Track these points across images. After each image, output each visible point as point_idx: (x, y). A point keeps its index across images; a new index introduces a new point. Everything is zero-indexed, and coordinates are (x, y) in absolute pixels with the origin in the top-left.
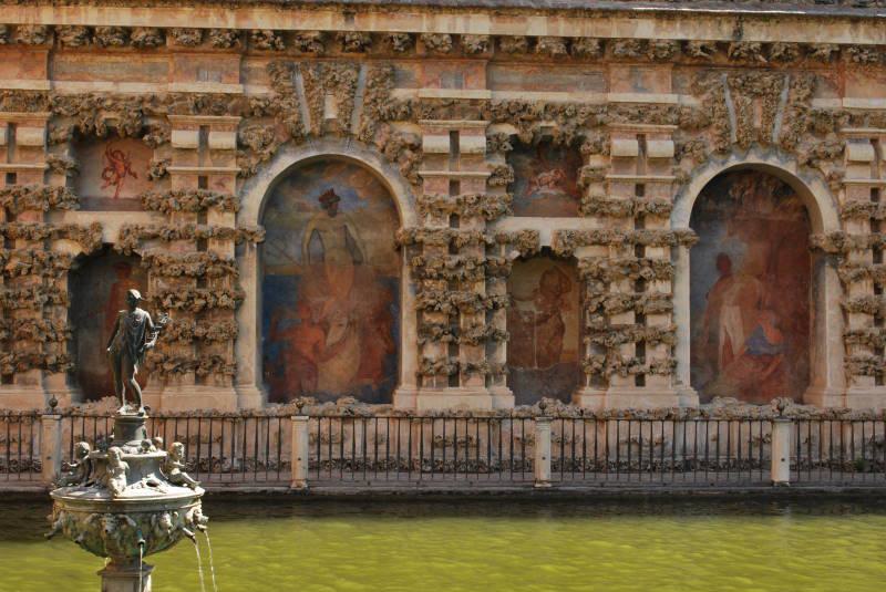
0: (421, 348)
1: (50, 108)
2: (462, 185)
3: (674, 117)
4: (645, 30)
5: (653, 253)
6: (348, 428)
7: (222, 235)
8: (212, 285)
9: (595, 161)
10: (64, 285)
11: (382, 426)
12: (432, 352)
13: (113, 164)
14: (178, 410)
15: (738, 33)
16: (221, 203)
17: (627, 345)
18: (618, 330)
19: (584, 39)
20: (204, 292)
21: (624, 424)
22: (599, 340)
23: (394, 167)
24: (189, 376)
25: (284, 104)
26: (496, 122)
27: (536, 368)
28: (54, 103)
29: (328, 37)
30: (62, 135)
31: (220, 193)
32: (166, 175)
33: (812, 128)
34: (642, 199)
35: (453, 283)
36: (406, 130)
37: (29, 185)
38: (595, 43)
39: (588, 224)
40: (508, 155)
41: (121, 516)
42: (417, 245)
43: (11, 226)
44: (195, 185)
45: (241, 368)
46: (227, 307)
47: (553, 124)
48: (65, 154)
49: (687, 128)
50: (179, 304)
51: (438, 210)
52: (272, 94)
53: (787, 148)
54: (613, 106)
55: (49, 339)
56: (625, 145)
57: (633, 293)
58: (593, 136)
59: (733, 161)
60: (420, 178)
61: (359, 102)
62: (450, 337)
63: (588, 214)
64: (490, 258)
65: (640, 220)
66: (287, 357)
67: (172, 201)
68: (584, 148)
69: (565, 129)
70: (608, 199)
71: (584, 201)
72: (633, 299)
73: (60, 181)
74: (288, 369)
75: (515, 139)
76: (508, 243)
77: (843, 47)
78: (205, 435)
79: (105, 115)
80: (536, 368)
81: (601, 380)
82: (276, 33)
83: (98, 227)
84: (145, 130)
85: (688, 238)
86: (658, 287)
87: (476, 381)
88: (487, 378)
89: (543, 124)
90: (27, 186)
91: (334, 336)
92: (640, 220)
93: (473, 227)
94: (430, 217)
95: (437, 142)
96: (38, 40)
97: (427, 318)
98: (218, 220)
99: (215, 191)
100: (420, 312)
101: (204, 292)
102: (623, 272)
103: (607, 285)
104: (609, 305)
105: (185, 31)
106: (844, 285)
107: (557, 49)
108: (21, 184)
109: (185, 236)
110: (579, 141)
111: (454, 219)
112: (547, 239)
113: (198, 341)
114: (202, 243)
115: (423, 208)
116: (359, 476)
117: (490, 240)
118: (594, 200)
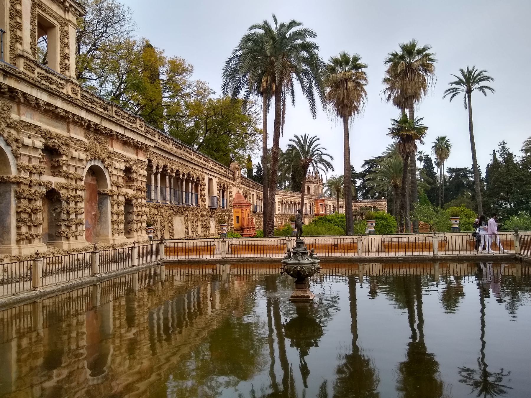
4: (83, 114)
9: (64, 158)
12: (24, 230)
15: (101, 122)
22: (66, 223)
23: (10, 148)
26: (42, 137)
33: (108, 157)
35: (30, 200)
38: (71, 115)
42: (18, 184)
47: (56, 141)
49: (86, 151)
53: (103, 162)
54: (71, 138)
57: (75, 207)
58: (64, 147)
59: (93, 164)
60: (20, 154)
70: (70, 172)
77: (117, 133)
81: (67, 238)
86: (80, 205)
94: (23, 172)
97: (24, 216)
100: (18, 213)
103: (68, 203)
104: (71, 211)
106: (112, 205)
111: (31, 173)
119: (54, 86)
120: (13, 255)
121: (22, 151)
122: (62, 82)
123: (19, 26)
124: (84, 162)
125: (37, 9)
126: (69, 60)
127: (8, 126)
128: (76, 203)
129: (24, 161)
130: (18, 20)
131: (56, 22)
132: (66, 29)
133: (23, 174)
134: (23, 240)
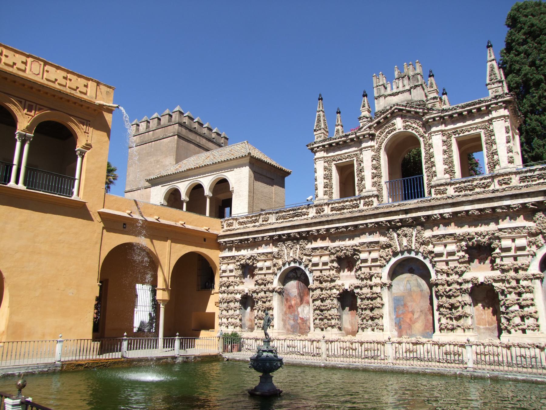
0: (439, 320)
1: (330, 251)
2: (449, 263)
3: (526, 231)
5: (522, 283)
6: (418, 346)
7: (375, 286)
8: (374, 301)
9: (498, 251)
10: (335, 301)
11: (429, 345)
12: (444, 321)
13: (349, 265)
14: (366, 340)
16: (376, 275)
17: (515, 318)
18: (512, 312)
19: (484, 209)
20: (372, 302)
21: (518, 349)
24: (370, 329)
25: (391, 243)
27: (487, 326)
29: (401, 220)
30: (333, 259)
31: (375, 272)
32: (360, 268)
34: (515, 262)
36: (430, 247)
37: (325, 274)
39: (497, 274)
40: (466, 252)
42: (437, 285)
44: (368, 269)
45: (384, 328)
46: (379, 308)
47: (479, 238)
48: (335, 264)
50: (365, 306)
51: (442, 272)
52: (388, 239)
54: (500, 230)
55: (332, 318)
56: (506, 243)
60: (435, 262)
61: (414, 239)
62: (450, 315)
63: (496, 270)
64: (461, 287)
65: (516, 270)
66: (402, 323)
67: (363, 276)
68: (492, 246)
69: (484, 240)
71: (494, 264)
72: (518, 300)
73: (333, 272)
74: (402, 326)
75: (467, 246)
76: (468, 282)
78: (376, 348)
79: (343, 252)
80: (487, 326)
82: (386, 221)
83: (343, 285)
84: (355, 254)
85: (538, 276)
86: (524, 296)
87: (459, 331)
88: (464, 331)
89: (476, 239)
91: (416, 316)
92: (516, 270)
93: (455, 277)
95: (438, 249)
96: (325, 233)
97: (441, 309)
98: (375, 281)
99: (374, 271)
101: (372, 302)
102: (511, 290)
103: (506, 296)
105: (362, 224)
107: (476, 213)
109: (366, 286)
110: (491, 243)
111: (448, 275)
112: (481, 280)
113: (372, 319)
114: (371, 287)
115: (437, 272)
116: (423, 363)
117: (460, 281)
118: (497, 265)
119: (477, 190)
120: (433, 340)
121: (436, 259)
122: (488, 180)
123: (433, 165)
124: (534, 248)
125: (453, 136)
126: (497, 155)
127: (423, 244)
128: (520, 294)
129: (441, 266)
130: (432, 160)
131: (478, 130)
132: (491, 128)
133: (440, 277)
134: (443, 329)
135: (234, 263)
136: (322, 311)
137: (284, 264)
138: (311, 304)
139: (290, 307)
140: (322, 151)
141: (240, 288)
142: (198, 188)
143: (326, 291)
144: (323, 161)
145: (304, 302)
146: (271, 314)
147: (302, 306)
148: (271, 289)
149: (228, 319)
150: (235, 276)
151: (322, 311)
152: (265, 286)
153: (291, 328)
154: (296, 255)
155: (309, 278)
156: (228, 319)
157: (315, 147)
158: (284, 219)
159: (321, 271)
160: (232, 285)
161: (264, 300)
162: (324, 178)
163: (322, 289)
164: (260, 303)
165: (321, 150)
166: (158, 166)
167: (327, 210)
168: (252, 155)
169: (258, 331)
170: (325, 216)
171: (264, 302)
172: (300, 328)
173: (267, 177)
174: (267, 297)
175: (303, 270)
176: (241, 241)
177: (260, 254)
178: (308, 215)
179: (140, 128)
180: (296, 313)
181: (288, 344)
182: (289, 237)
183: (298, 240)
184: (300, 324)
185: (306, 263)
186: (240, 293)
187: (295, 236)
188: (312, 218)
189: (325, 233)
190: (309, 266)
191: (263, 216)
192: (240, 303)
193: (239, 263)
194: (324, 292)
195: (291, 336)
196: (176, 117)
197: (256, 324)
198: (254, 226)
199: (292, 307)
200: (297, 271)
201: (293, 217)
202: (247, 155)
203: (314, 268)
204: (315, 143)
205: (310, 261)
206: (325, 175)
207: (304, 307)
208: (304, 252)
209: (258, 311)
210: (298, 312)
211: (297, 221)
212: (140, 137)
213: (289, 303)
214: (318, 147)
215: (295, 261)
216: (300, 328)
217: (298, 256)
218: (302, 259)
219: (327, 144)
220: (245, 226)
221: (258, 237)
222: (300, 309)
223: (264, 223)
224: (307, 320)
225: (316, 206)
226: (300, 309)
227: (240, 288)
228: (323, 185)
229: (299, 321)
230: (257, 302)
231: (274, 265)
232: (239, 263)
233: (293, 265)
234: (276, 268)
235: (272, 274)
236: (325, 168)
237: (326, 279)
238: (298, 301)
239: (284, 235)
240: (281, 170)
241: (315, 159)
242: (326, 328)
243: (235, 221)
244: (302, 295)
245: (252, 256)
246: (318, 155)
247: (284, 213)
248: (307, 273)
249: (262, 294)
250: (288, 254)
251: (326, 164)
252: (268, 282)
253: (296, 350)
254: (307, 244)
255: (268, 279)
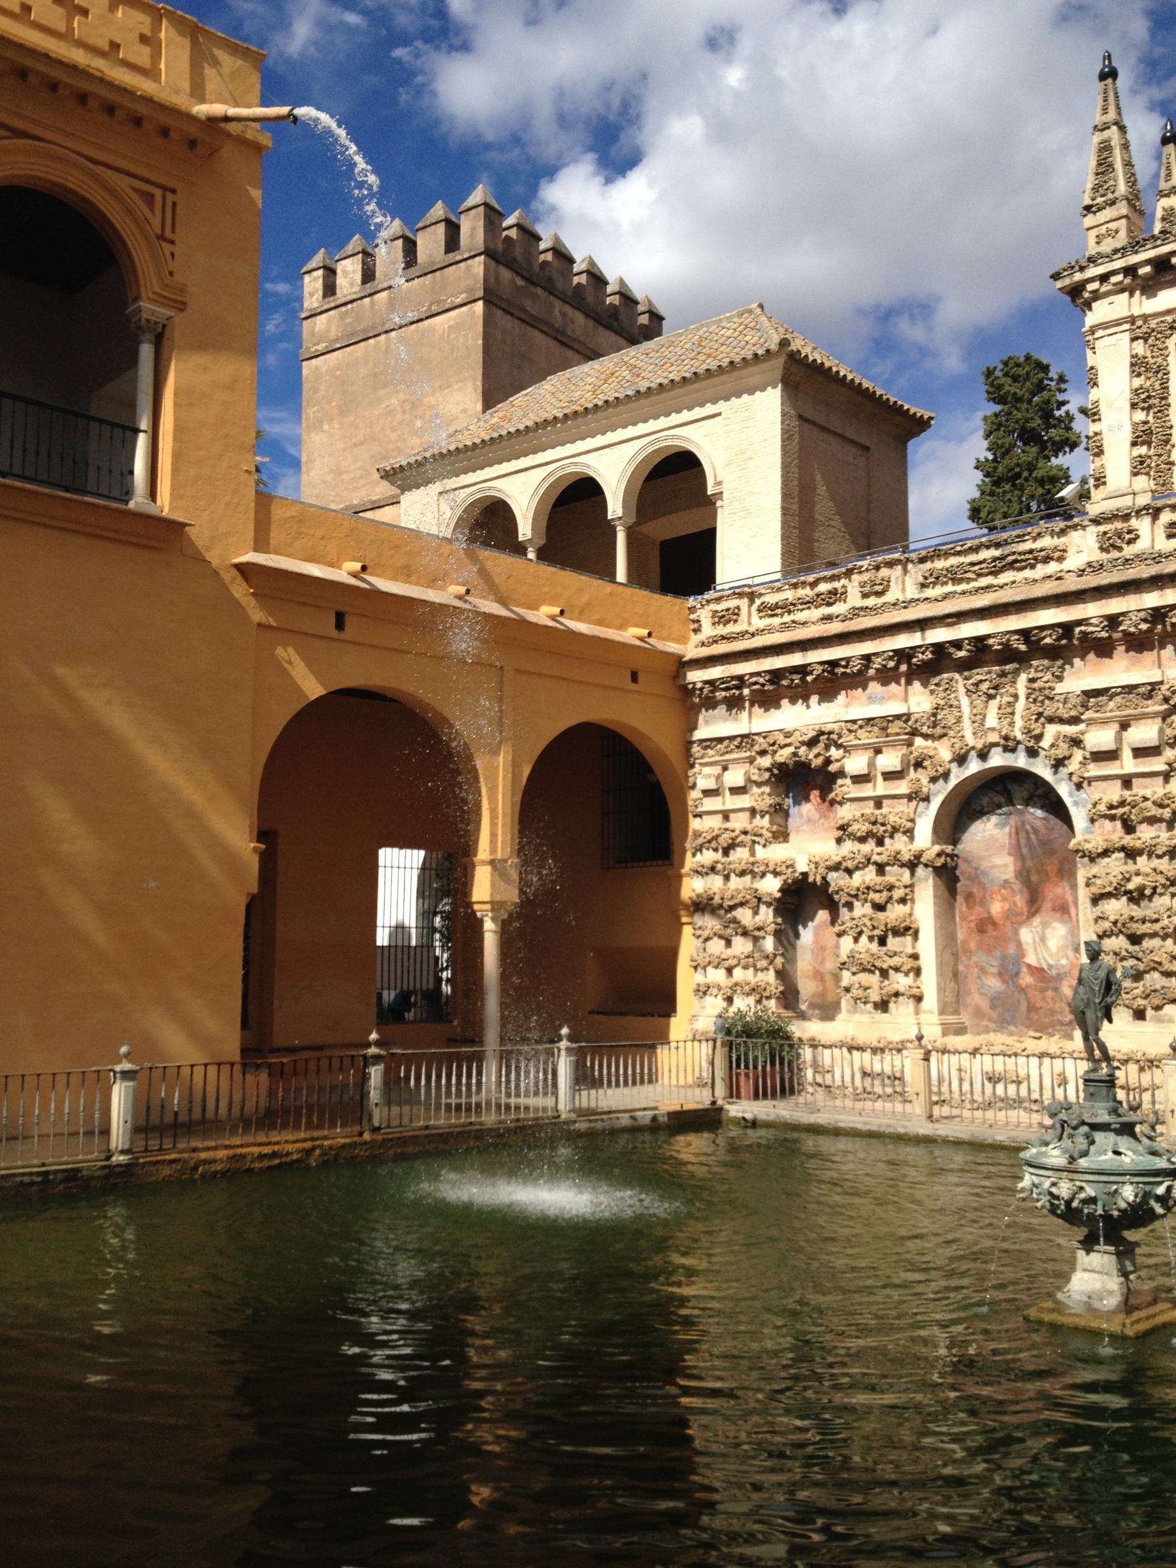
1: (1166, 700)
28: (1168, 694)
37: (1148, 793)
41: (1078, 1183)
43: (1128, 840)
90: (1141, 793)
108: (1141, 788)
135: (751, 761)
136: (1135, 939)
137: (961, 760)
138: (1085, 911)
139: (984, 925)
140: (1122, 291)
141: (775, 853)
142: (580, 494)
143: (1155, 862)
144: (1127, 336)
145: (1047, 905)
146: (909, 951)
147: (1037, 921)
148: (906, 857)
149: (729, 971)
150: (753, 812)
151: (1135, 939)
152: (880, 842)
153: (993, 1007)
154: (1012, 724)
155: (1073, 811)
156: (729, 971)
157: (1091, 280)
158: (956, 581)
159: (1127, 782)
160: (742, 844)
161: (878, 898)
162: (1134, 406)
163: (1131, 854)
164: (861, 910)
165: (1120, 289)
166: (418, 423)
167: (1150, 536)
168: (794, 347)
169: (857, 1017)
170: (1140, 558)
171: (880, 908)
172: (1032, 1008)
173: (844, 438)
174: (891, 888)
175: (1045, 783)
176: (776, 675)
177: (854, 722)
178: (1061, 559)
179: (341, 281)
180: (1012, 949)
181: (988, 1067)
182: (982, 651)
183: (1022, 660)
184: (1032, 994)
185: (1061, 752)
186: (776, 874)
187: (1007, 646)
188: (1081, 573)
189: (1144, 626)
190: (1073, 765)
191: (866, 577)
192: (777, 912)
193: (766, 761)
194: (1142, 862)
195: (999, 1040)
196: (473, 229)
197: (847, 990)
198: (828, 618)
199: (994, 924)
200: (1014, 788)
201: (995, 573)
202: (774, 347)
203: (1094, 770)
204: (1092, 260)
205: (1076, 742)
206: (1136, 392)
207: (1045, 925)
208: (1050, 709)
209: (856, 940)
210: (1019, 944)
211: (1014, 584)
212: (342, 317)
213: (978, 909)
214: (1104, 278)
215: (1009, 746)
216: (1032, 1008)
217: (1019, 723)
218: (1039, 737)
219: (1148, 262)
220: (787, 618)
221: (848, 660)
222: (1026, 935)
223: (871, 601)
224: (1060, 977)
225: (1096, 522)
226: (1026, 935)
227: (775, 853)
228: (1127, 435)
229: (1026, 979)
230: (850, 906)
231: (918, 765)
232: (766, 761)
233: (997, 759)
234: (923, 776)
235: (910, 797)
236: (1138, 366)
237: (1155, 811)
238: (1020, 901)
239: (957, 644)
240: (897, 410)
241: (1093, 330)
242: (1158, 1008)
243: (744, 603)
244: (1034, 878)
245: (823, 733)
246: (1101, 312)
247: (953, 561)
248: (1064, 790)
249: (868, 876)
250: (979, 720)
251: (1140, 348)
252: (895, 830)
253: (1024, 1092)
254: (1060, 678)
255: (892, 819)
